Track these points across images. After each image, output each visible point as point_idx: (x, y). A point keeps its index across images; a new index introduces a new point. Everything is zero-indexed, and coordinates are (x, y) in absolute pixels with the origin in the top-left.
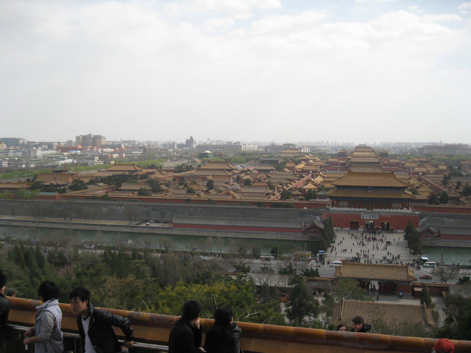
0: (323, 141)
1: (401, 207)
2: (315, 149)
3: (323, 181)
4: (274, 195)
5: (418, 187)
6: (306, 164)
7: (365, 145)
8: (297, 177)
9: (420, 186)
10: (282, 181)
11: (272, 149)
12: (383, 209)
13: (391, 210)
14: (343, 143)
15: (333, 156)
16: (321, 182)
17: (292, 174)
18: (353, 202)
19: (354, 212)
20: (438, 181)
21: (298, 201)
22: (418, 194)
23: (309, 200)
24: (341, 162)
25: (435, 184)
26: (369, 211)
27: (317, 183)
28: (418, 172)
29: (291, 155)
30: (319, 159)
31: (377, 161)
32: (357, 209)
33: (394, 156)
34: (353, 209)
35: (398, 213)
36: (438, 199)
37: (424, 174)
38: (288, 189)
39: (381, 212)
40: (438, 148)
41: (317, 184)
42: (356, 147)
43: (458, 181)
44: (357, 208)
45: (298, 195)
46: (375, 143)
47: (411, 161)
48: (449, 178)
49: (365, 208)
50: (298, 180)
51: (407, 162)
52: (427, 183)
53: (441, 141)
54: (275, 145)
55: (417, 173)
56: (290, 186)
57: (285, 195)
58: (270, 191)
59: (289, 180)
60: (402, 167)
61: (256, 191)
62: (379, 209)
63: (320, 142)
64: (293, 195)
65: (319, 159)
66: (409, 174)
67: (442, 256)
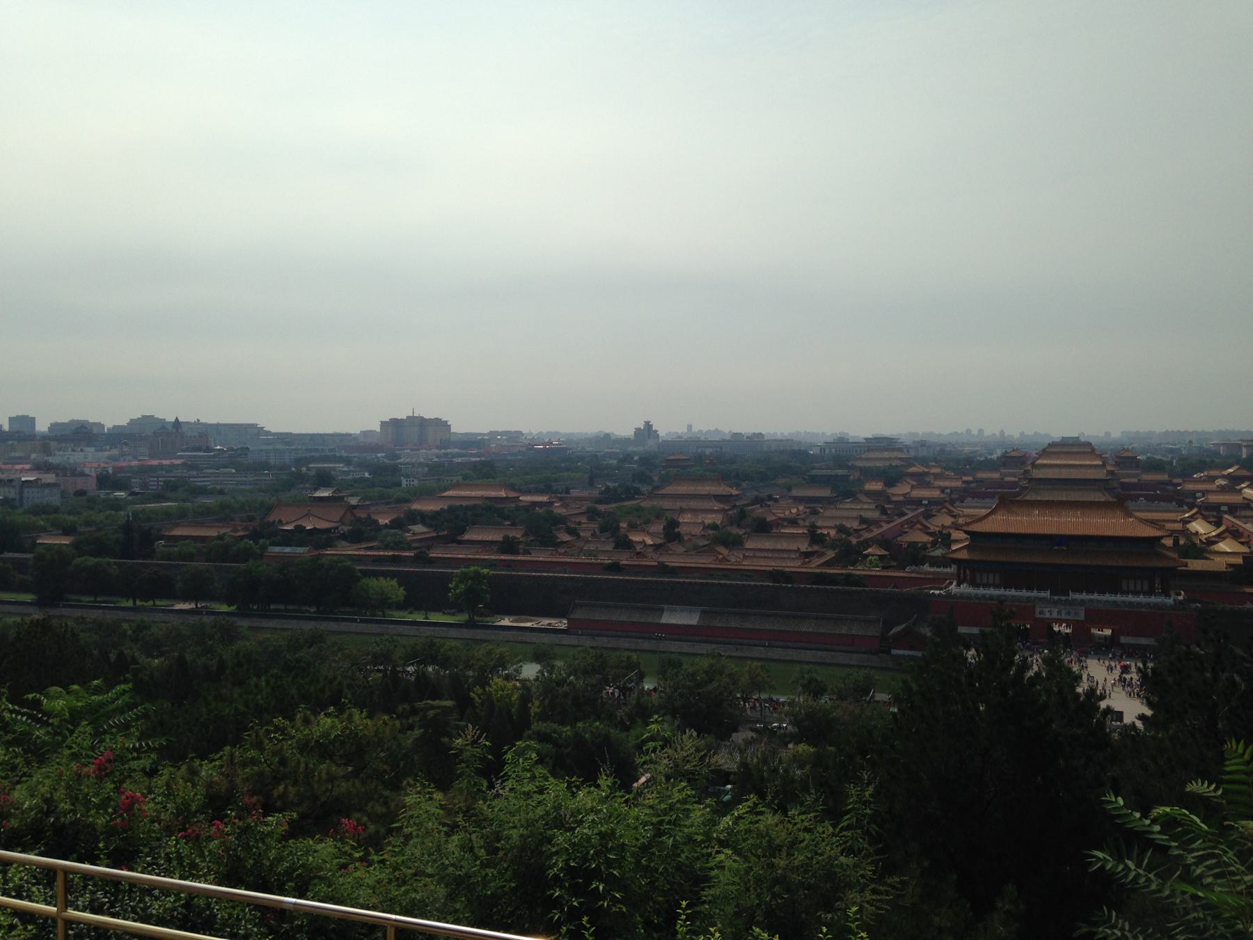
0: (968, 431)
4: (821, 555)
10: (848, 525)
14: (1022, 434)
17: (873, 506)
18: (1012, 576)
22: (1206, 558)
23: (904, 568)
29: (878, 464)
31: (1101, 474)
34: (1013, 592)
46: (1108, 434)
49: (1045, 589)
55: (1216, 507)
56: (867, 535)
57: (850, 554)
58: (816, 548)
59: (863, 521)
61: (779, 547)
66: (1191, 509)
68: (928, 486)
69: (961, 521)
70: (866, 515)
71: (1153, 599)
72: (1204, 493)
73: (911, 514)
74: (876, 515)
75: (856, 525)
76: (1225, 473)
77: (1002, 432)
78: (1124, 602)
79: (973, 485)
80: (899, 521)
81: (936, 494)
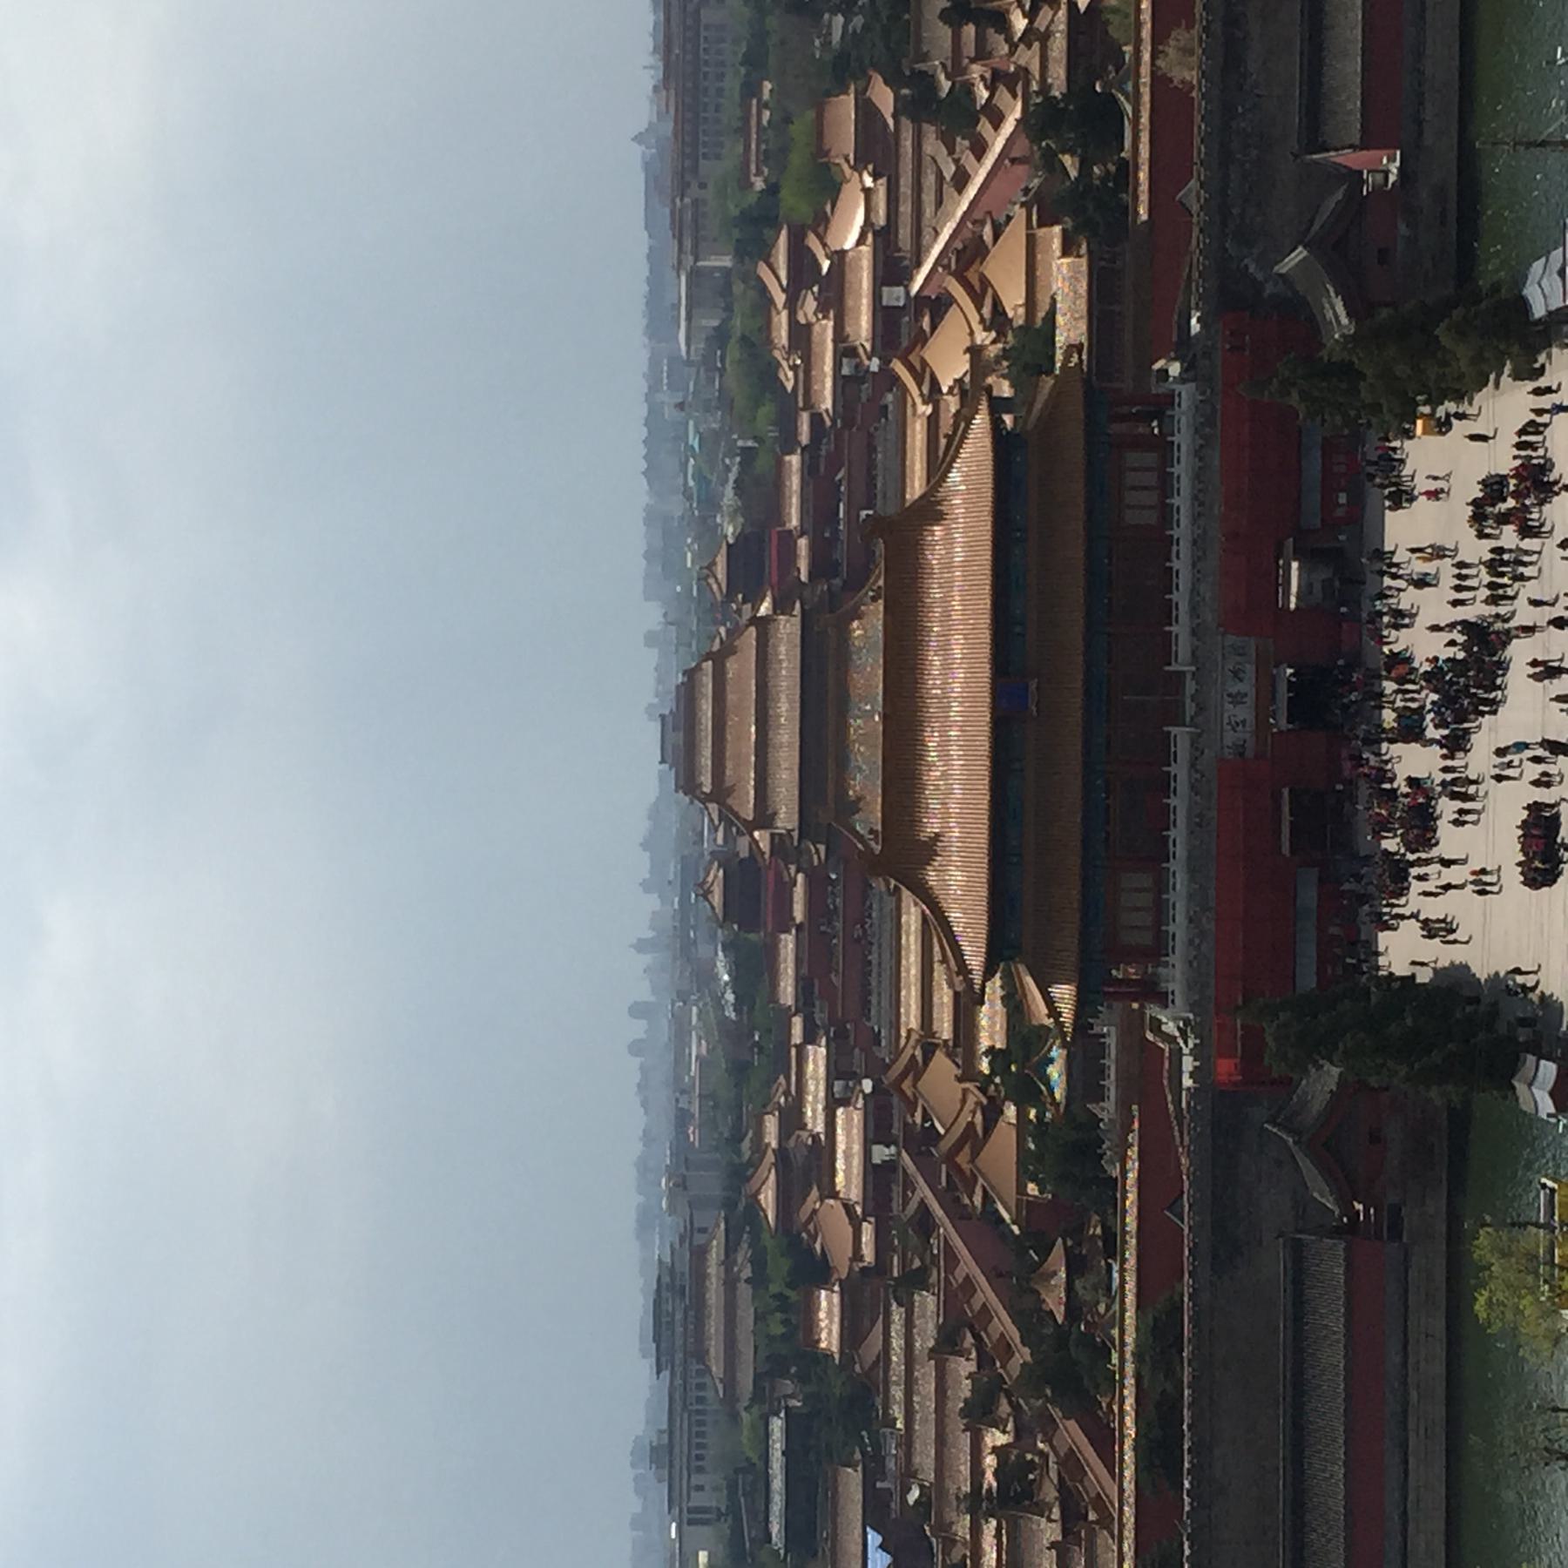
0: (636, 1048)
1: (1151, 458)
2: (695, 1109)
3: (950, 1055)
5: (998, 320)
6: (815, 1193)
7: (663, 717)
8: (924, 1271)
9: (988, 302)
11: (696, 1463)
12: (1175, 596)
13: (1183, 530)
14: (647, 886)
15: (754, 970)
16: (960, 1080)
19: (1197, 824)
20: (949, 170)
21: (1122, 1271)
24: (799, 913)
25: (972, 191)
26: (1190, 708)
27: (970, 1104)
28: (879, 314)
30: (782, 1079)
32: (1179, 803)
33: (760, 494)
35: (1198, 476)
36: (1085, 167)
37: (891, 269)
38: (1027, 1351)
39: (1194, 610)
40: (687, 163)
41: (978, 1103)
42: (687, 784)
43: (945, 16)
44: (1173, 801)
45: (1075, 1267)
46: (651, 639)
47: (794, 368)
48: (926, 82)
50: (952, 1258)
51: (801, 404)
52: (968, 255)
53: (638, 139)
54: (666, 1441)
55: (885, 318)
57: (1069, 1370)
59: (947, 1344)
60: (838, 436)
62: (1174, 629)
63: (643, 1069)
64: (1074, 1308)
65: (782, 1079)
66: (896, 379)
67: (1543, 144)
68: (823, 1151)
69: (944, 1028)
70: (926, 1338)
71: (1183, 439)
72: (845, 350)
73: (924, 1191)
74: (927, 1303)
75: (964, 1367)
76: (780, 298)
77: (641, 946)
78: (1196, 518)
79: (820, 1017)
80: (946, 1227)
81: (849, 1129)
